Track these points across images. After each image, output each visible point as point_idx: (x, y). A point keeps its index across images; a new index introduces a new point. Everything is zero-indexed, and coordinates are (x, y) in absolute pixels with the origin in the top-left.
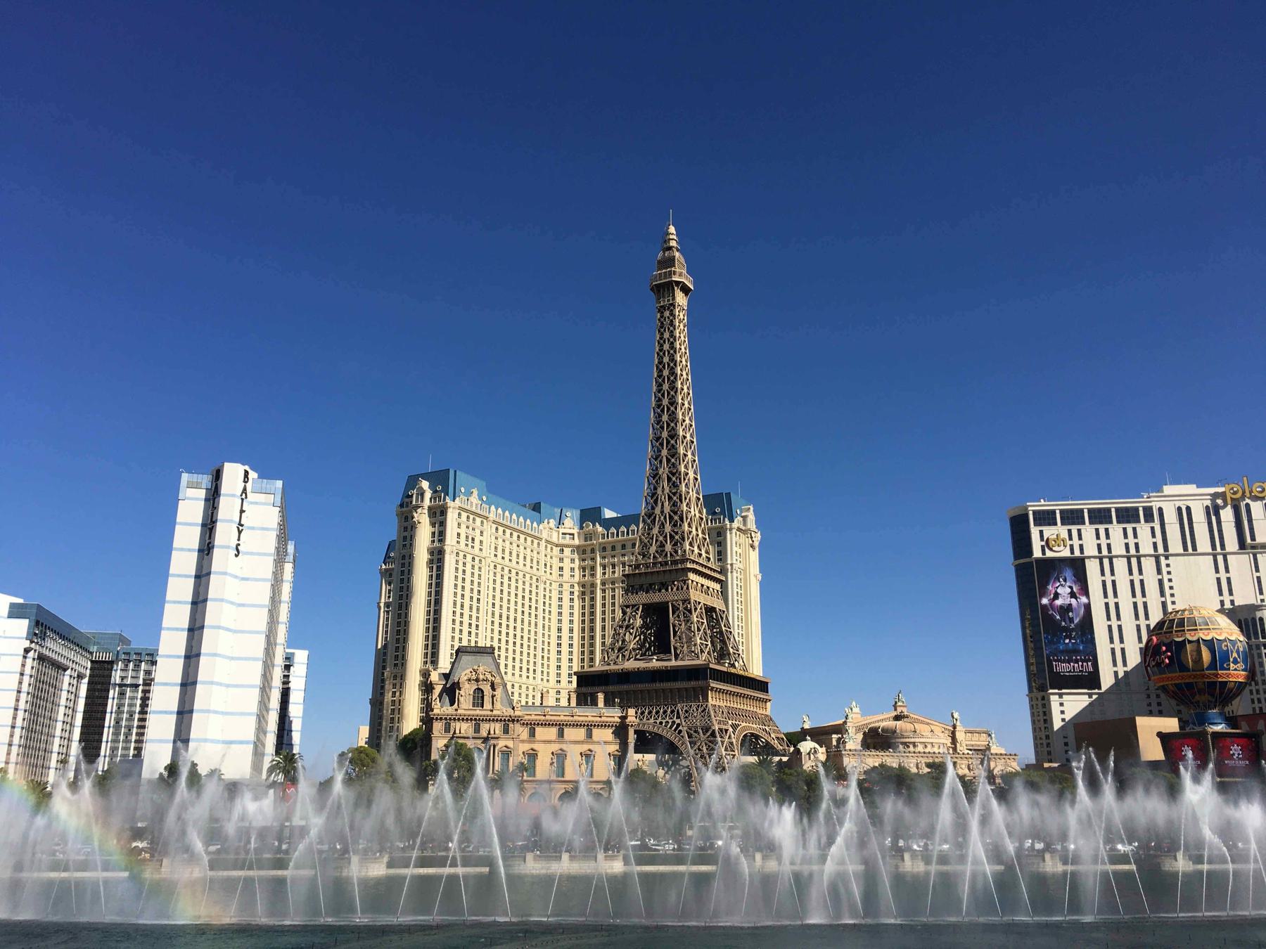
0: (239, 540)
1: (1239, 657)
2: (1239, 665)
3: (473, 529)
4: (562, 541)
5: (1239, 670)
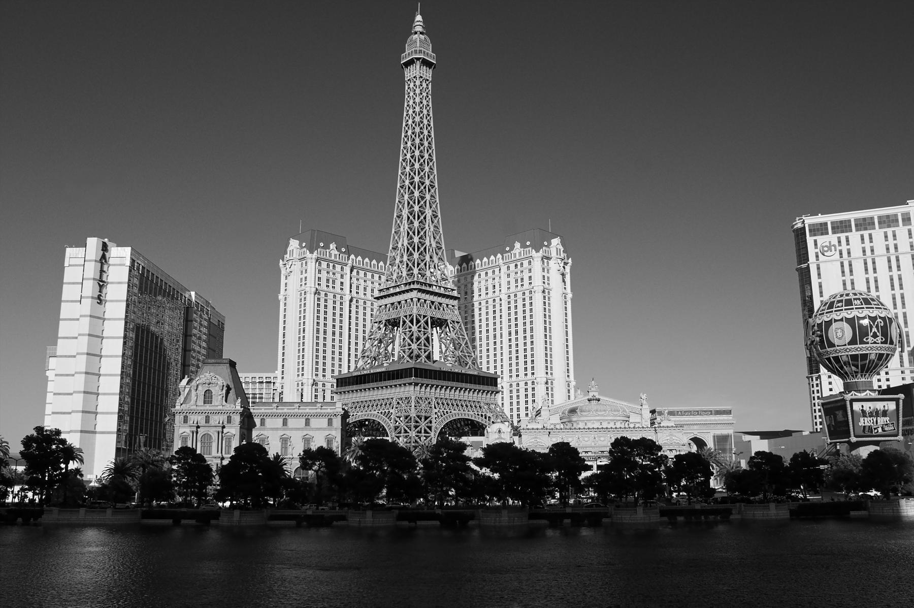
0: (100, 291)
2: (878, 338)
3: (334, 274)
5: (879, 343)
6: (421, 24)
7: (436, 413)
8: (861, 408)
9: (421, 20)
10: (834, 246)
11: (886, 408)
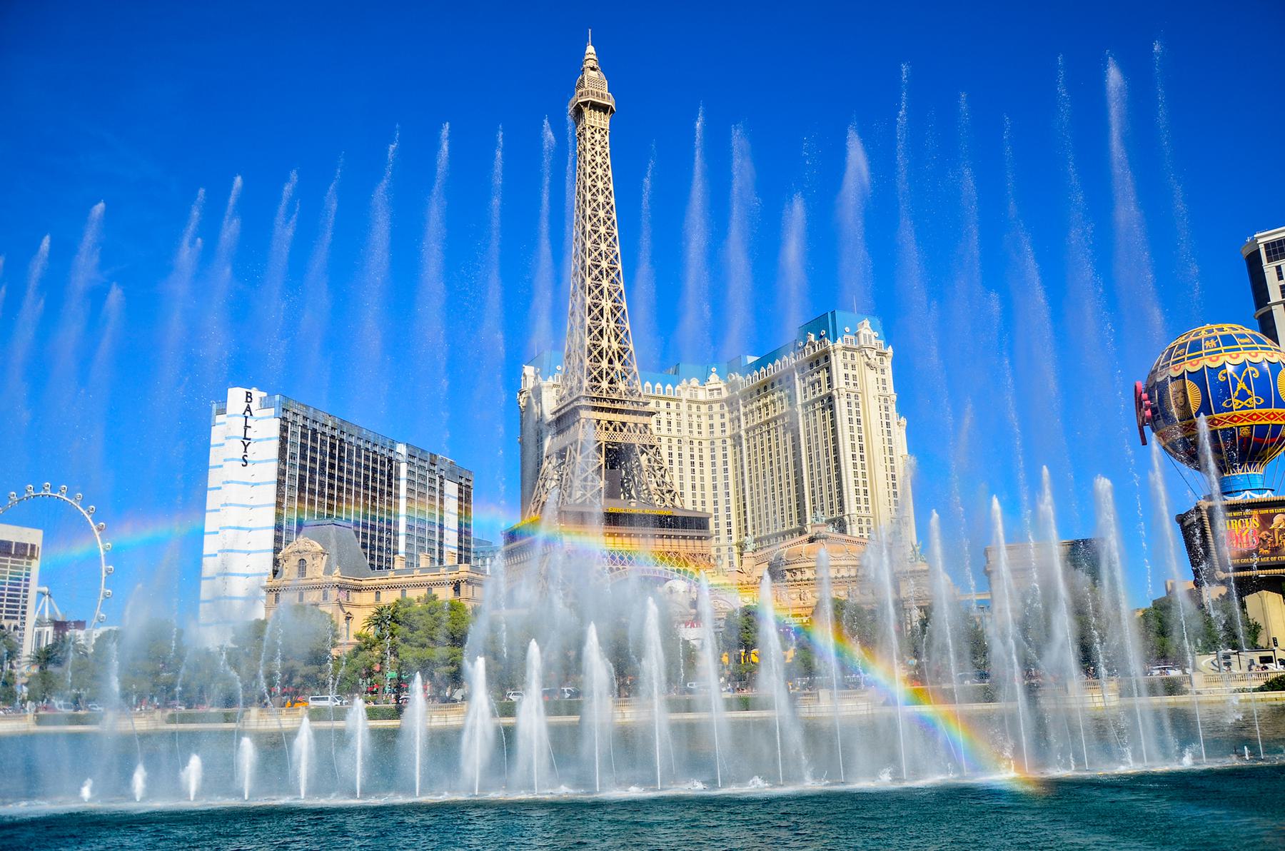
0: (245, 451)
1: (1249, 388)
2: (1250, 400)
4: (709, 398)
6: (595, 57)
7: (598, 572)
9: (594, 53)
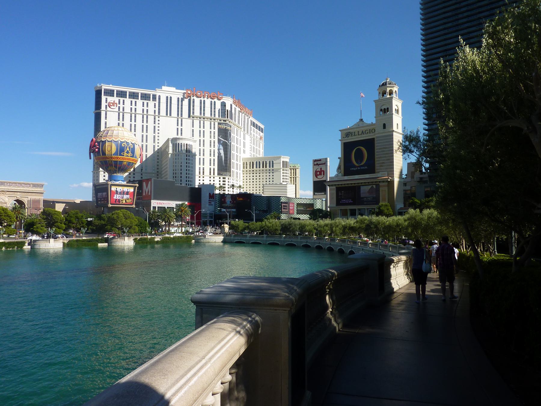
5: (129, 157)
8: (116, 190)
10: (116, 104)
11: (129, 191)
